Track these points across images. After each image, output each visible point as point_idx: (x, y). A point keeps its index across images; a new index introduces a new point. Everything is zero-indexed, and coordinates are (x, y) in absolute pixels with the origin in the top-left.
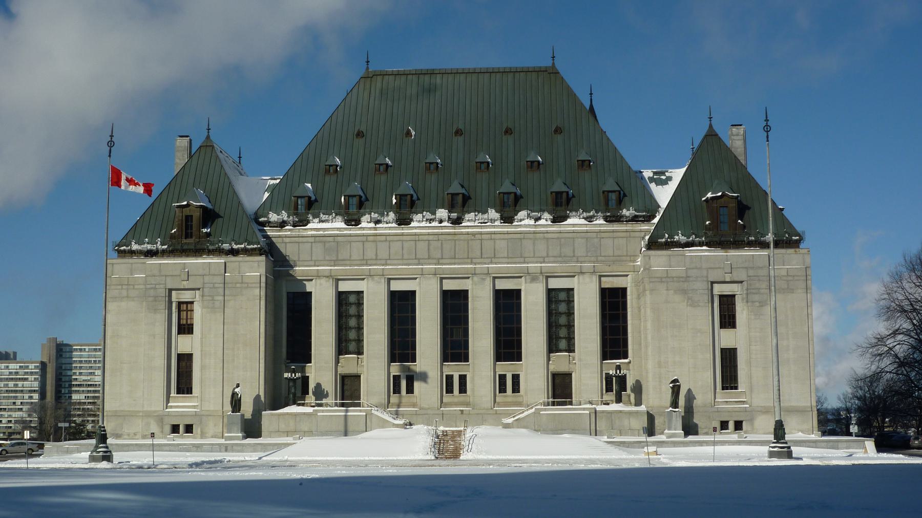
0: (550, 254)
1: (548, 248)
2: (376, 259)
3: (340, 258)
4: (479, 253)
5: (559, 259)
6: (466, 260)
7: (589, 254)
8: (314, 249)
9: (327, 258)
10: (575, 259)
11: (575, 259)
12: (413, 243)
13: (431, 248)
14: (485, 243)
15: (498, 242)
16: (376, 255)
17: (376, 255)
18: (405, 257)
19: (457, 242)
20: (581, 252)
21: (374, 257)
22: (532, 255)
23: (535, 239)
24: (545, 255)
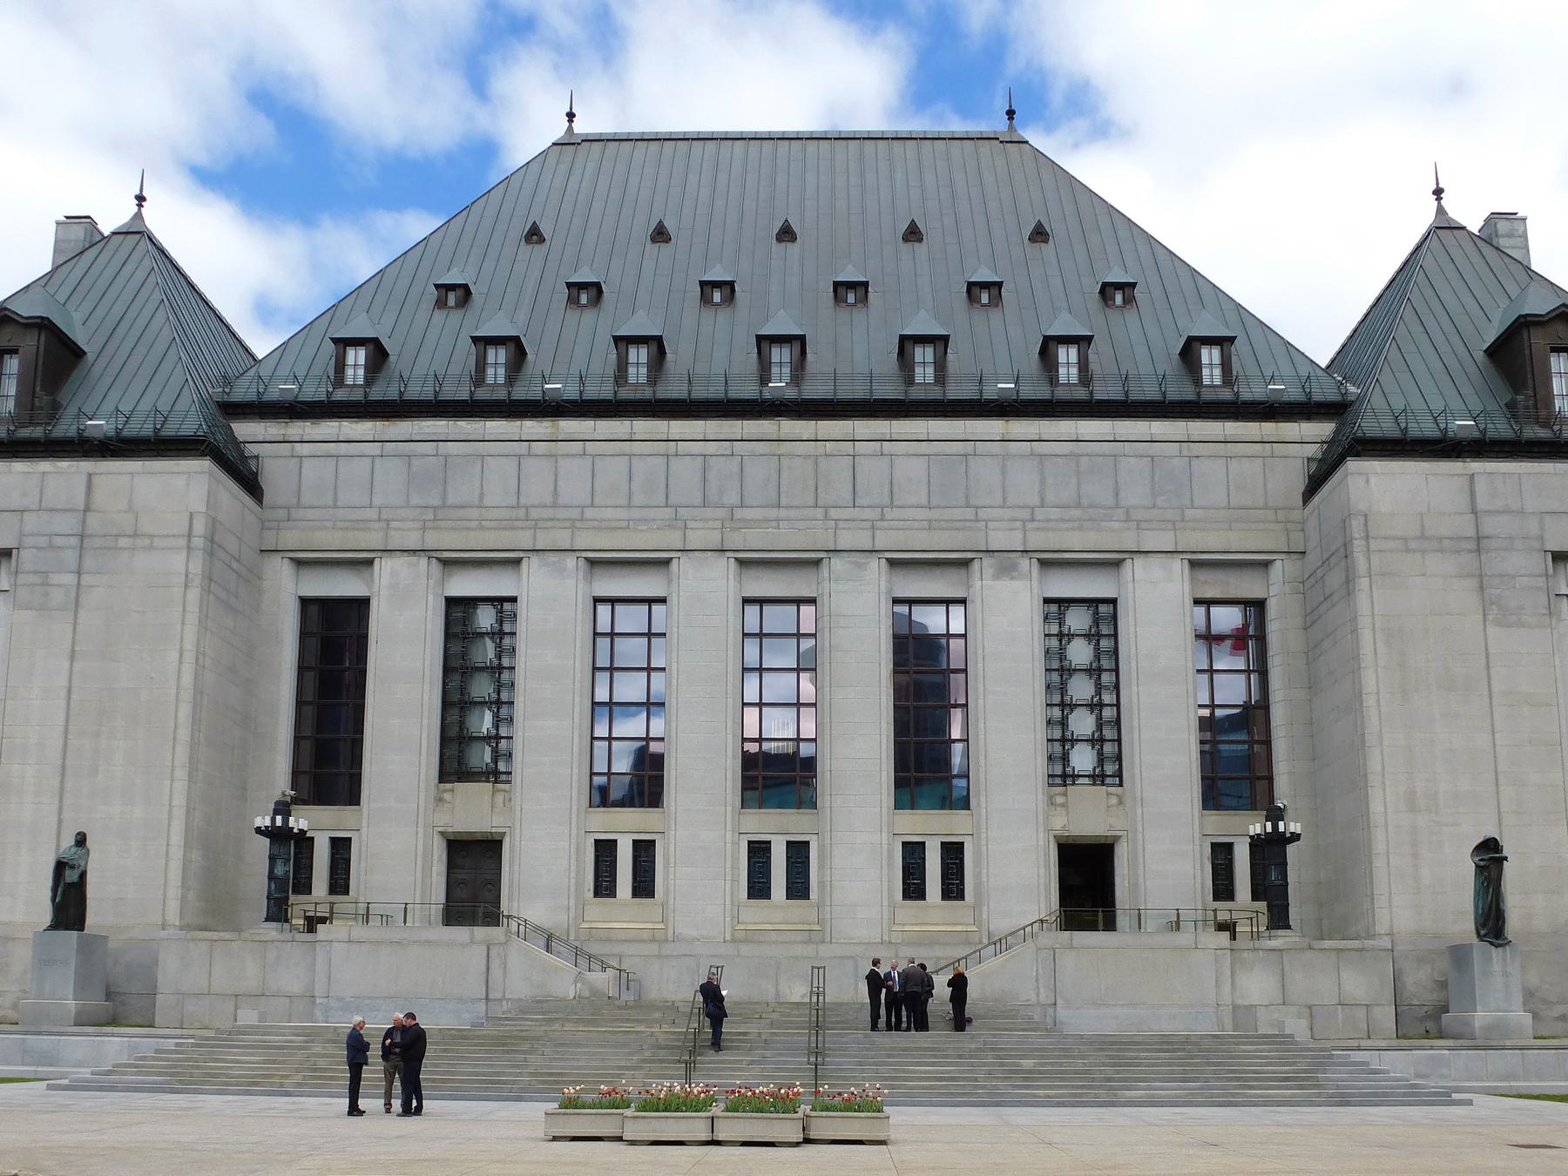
0: (1050, 498)
1: (1043, 482)
2: (555, 506)
3: (451, 500)
4: (849, 497)
5: (1076, 513)
6: (811, 513)
7: (1160, 501)
8: (378, 476)
9: (415, 501)
10: (1120, 513)
11: (1120, 513)
12: (662, 460)
13: (711, 476)
14: (864, 465)
15: (898, 461)
16: (555, 492)
17: (555, 492)
18: (638, 499)
19: (785, 461)
20: (1135, 495)
21: (548, 500)
22: (999, 501)
23: (1006, 457)
24: (1037, 501)
